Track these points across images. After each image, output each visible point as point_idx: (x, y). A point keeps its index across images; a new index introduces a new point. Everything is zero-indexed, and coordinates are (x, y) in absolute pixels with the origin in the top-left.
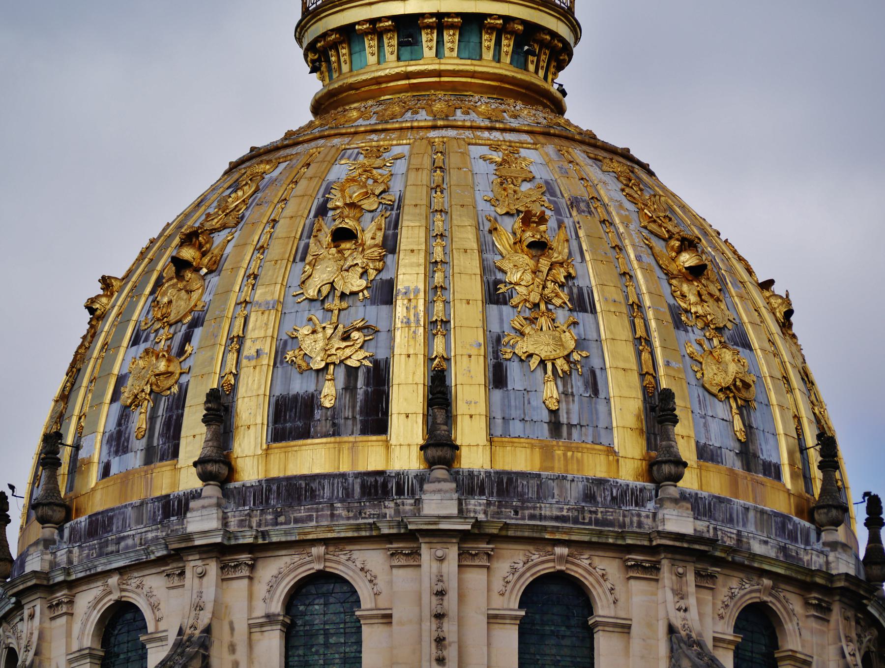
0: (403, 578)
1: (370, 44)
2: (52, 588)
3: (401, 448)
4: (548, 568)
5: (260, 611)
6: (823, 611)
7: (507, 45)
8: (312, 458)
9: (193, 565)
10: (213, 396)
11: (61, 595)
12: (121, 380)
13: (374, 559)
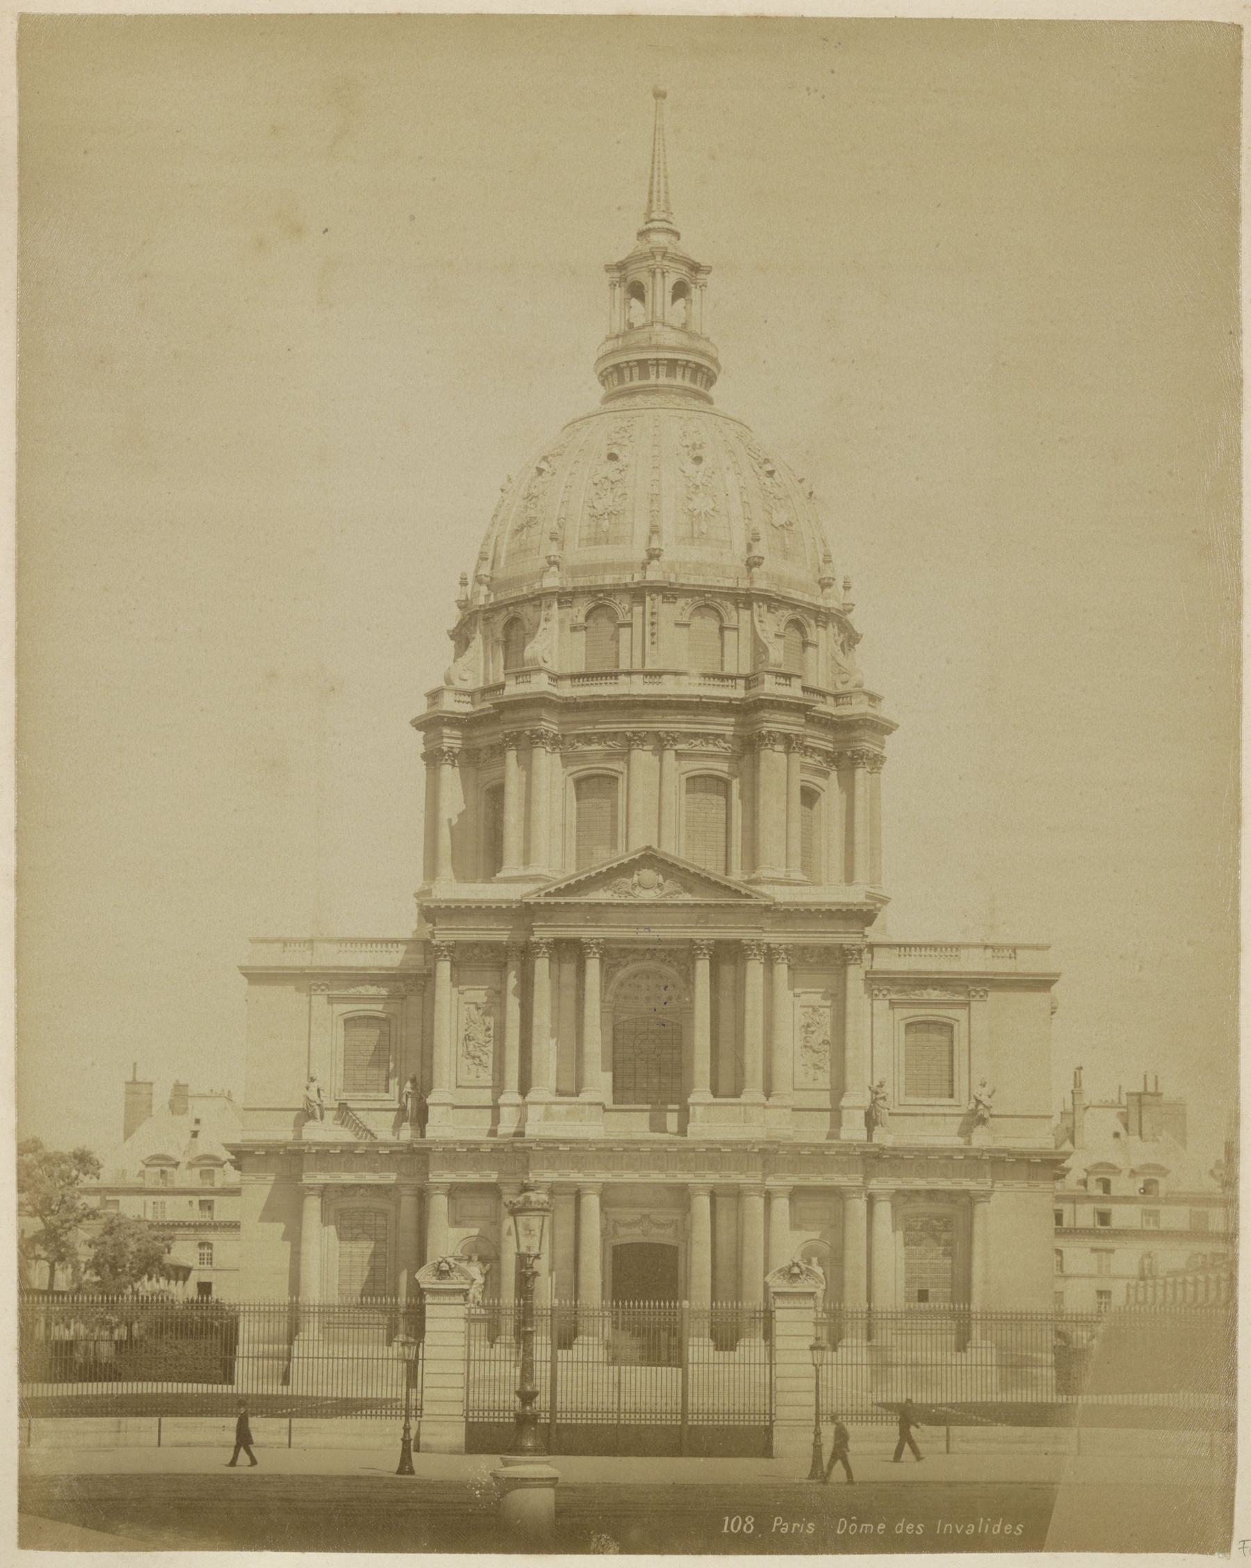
0: (638, 609)
1: (627, 373)
7: (688, 375)
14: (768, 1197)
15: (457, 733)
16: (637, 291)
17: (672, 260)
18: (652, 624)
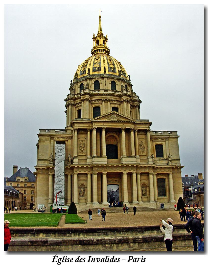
2: (77, 83)
3: (102, 72)
4: (113, 80)
5: (92, 83)
6: (130, 86)
7: (106, 52)
8: (96, 73)
9: (87, 80)
10: (88, 69)
11: (77, 83)
12: (81, 69)
13: (100, 79)
14: (137, 174)
15: (73, 101)
16: (98, 42)
17: (103, 37)
18: (105, 83)
